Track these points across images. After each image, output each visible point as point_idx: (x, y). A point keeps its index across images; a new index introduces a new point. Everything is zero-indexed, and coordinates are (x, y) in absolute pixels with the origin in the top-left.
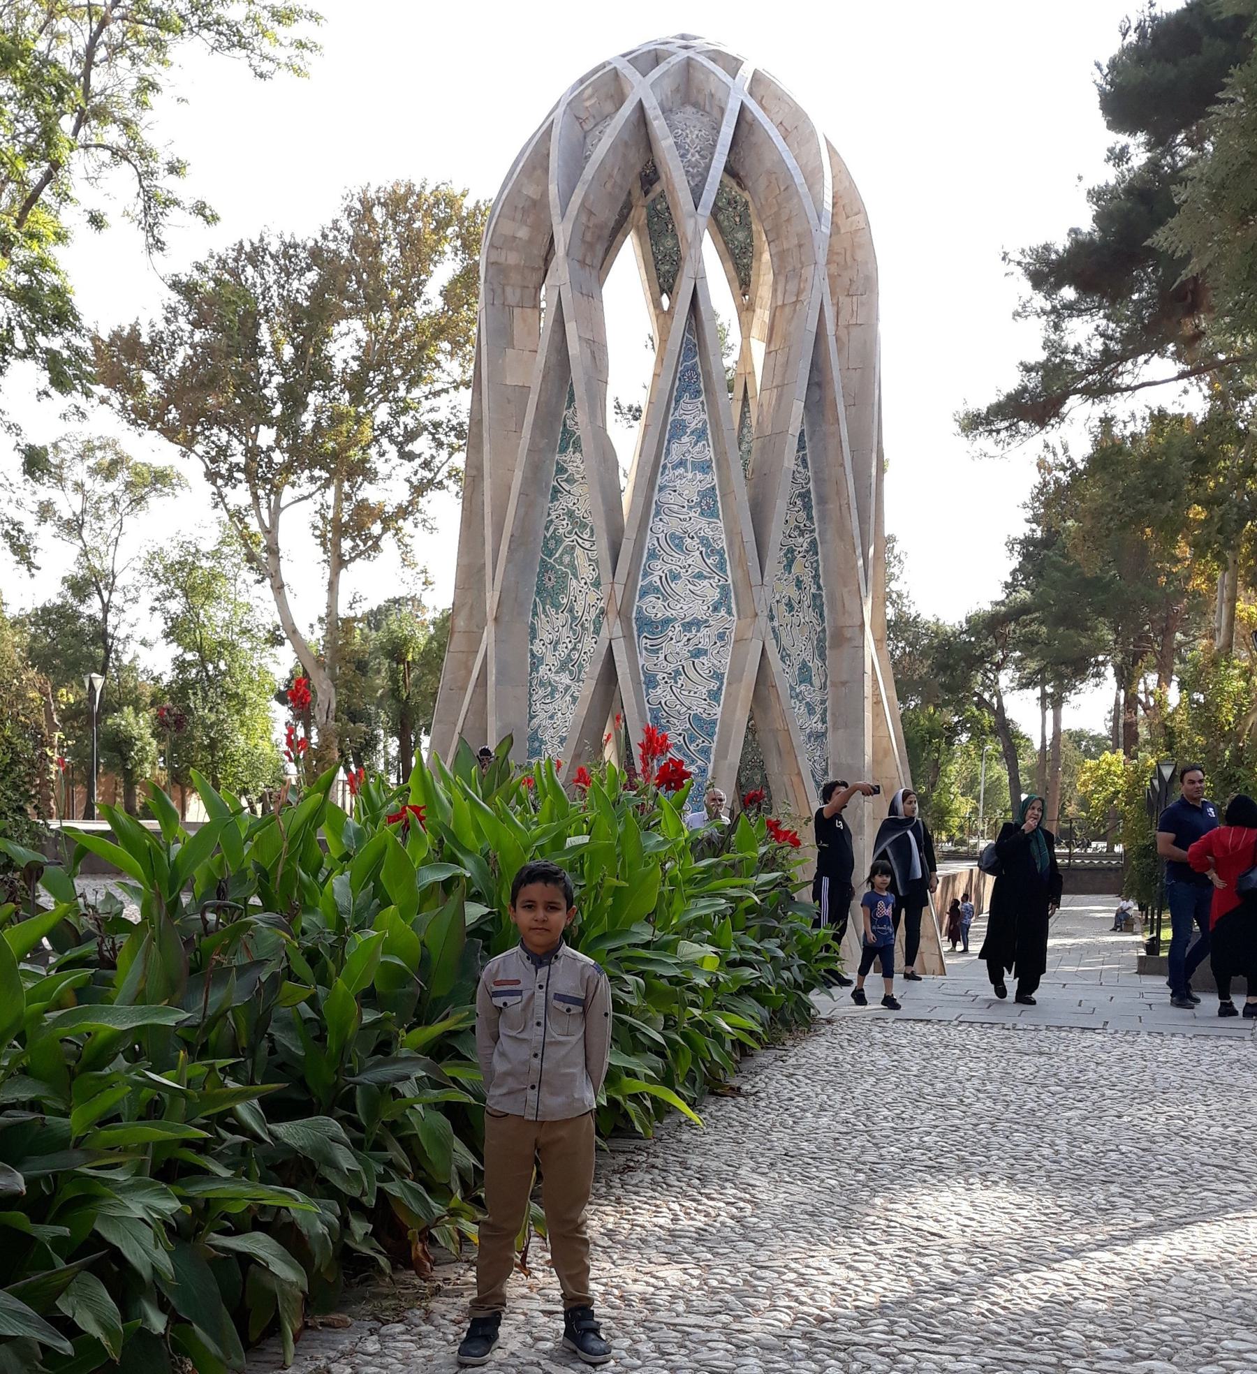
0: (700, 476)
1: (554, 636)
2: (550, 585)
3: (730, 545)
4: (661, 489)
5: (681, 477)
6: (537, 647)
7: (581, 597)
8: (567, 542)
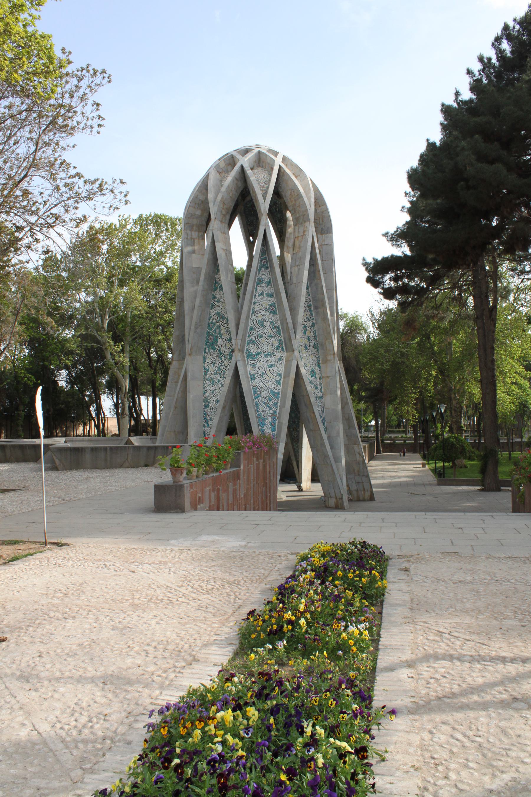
0: (269, 299)
1: (213, 361)
2: (211, 341)
3: (282, 324)
4: (254, 304)
5: (262, 299)
6: (206, 365)
7: (223, 346)
8: (217, 324)
